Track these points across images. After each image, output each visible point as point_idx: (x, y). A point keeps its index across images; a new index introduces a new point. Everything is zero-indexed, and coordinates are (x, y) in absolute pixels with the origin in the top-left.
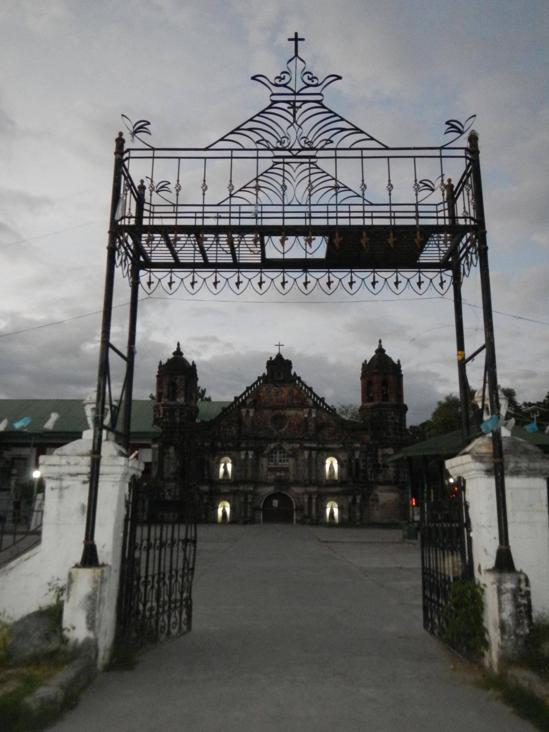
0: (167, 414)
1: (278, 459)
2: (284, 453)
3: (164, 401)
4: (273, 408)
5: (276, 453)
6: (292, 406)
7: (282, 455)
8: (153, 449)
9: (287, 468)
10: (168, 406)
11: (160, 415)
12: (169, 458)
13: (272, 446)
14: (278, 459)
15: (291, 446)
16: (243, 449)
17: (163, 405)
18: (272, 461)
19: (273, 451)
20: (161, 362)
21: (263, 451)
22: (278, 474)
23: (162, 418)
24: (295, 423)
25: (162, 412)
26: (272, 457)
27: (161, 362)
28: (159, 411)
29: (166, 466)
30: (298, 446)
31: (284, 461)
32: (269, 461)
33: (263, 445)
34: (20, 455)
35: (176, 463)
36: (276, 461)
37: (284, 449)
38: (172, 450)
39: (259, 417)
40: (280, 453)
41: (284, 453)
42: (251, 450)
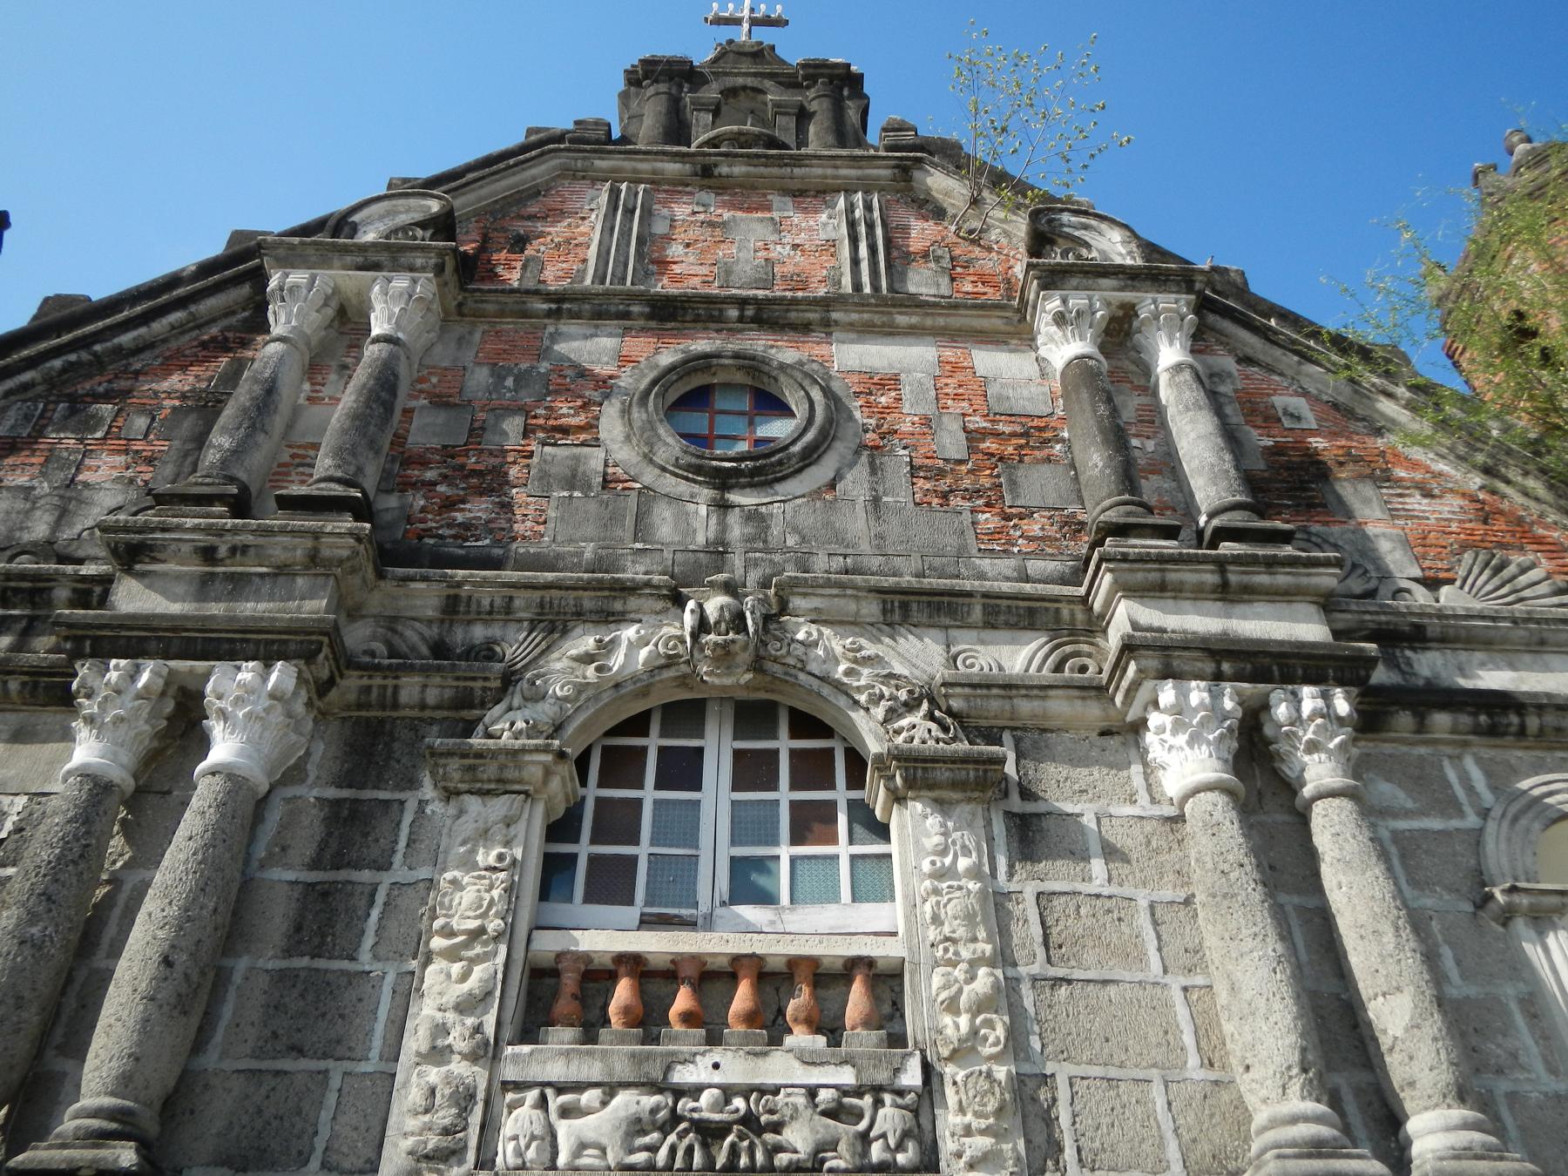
1: (715, 848)
2: (812, 770)
4: (670, 313)
5: (683, 770)
6: (886, 310)
7: (784, 795)
9: (886, 982)
13: (635, 646)
14: (715, 848)
15: (919, 655)
16: (137, 639)
18: (611, 883)
19: (638, 740)
21: (464, 713)
22: (711, 1071)
24: (951, 443)
26: (619, 822)
30: (1019, 656)
31: (814, 886)
32: (555, 872)
33: (479, 633)
36: (676, 876)
37: (805, 724)
39: (480, 377)
40: (752, 771)
41: (812, 770)
42: (262, 645)
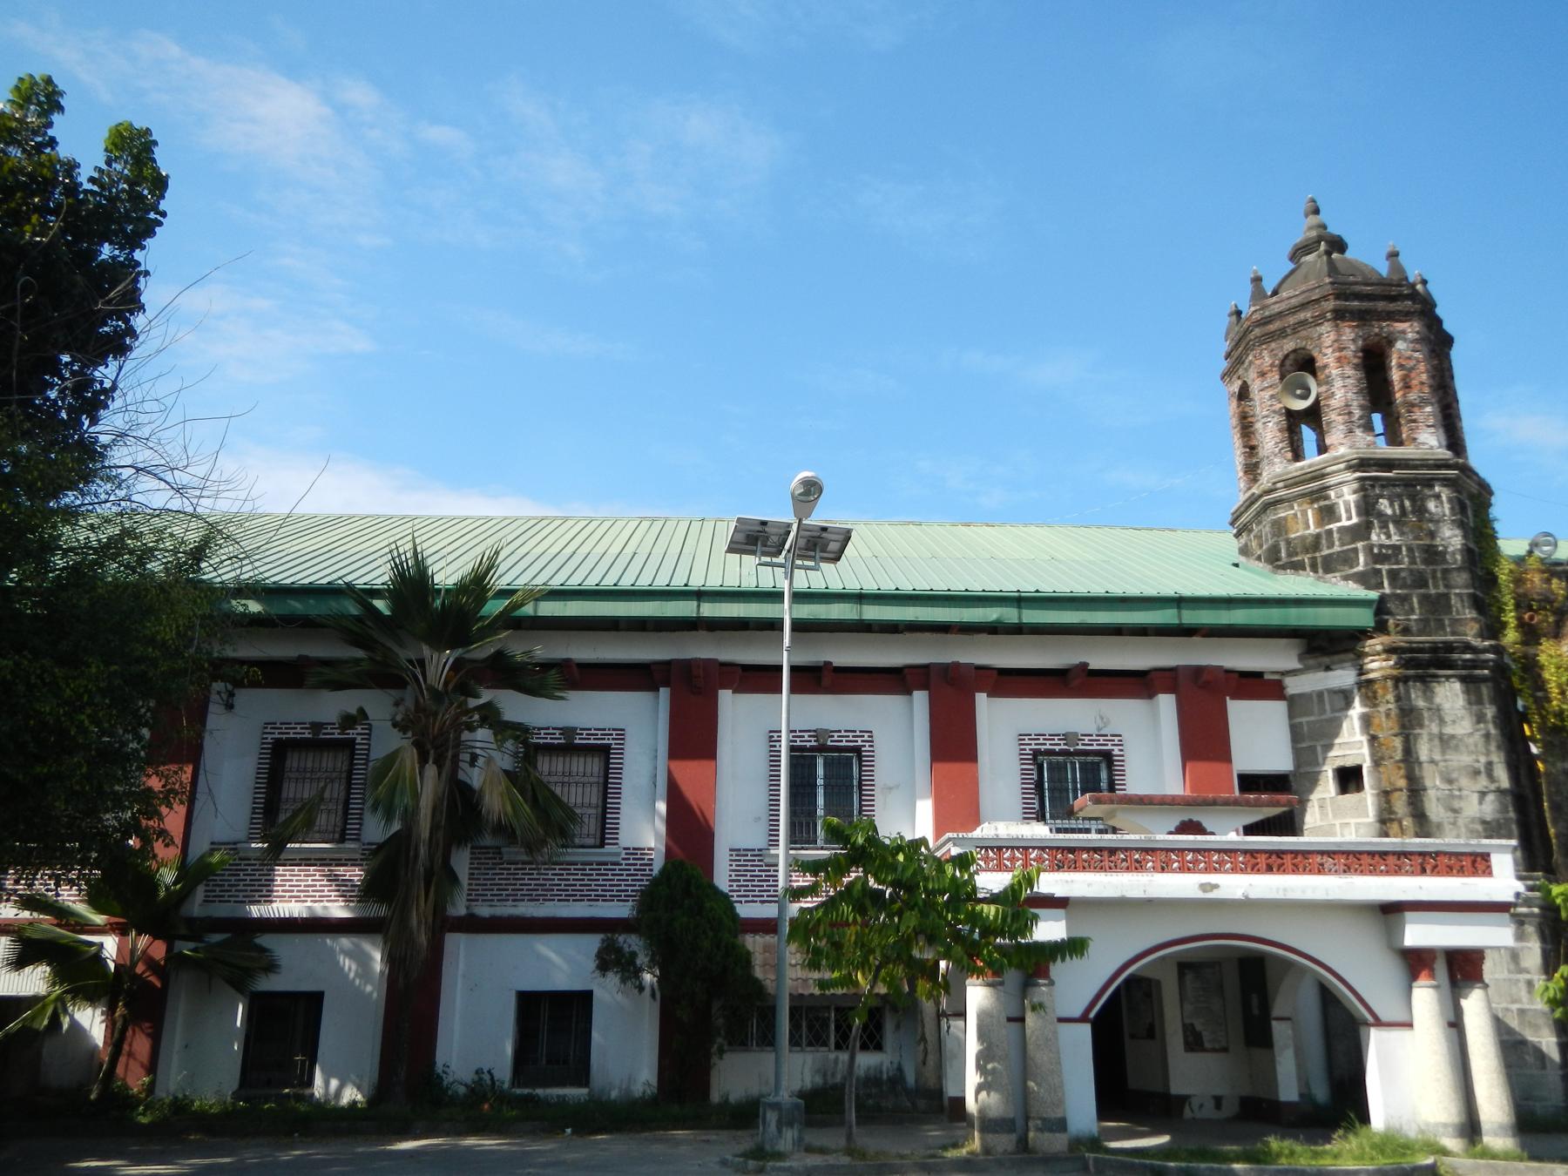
0: (1384, 506)
3: (1343, 444)
8: (1296, 705)
10: (1387, 464)
11: (1329, 513)
12: (1445, 742)
17: (1363, 464)
20: (1257, 280)
23: (1361, 532)
25: (1346, 497)
27: (1257, 280)
28: (1319, 495)
29: (1433, 783)
34: (569, 732)
35: (1489, 765)
38: (1450, 695)
